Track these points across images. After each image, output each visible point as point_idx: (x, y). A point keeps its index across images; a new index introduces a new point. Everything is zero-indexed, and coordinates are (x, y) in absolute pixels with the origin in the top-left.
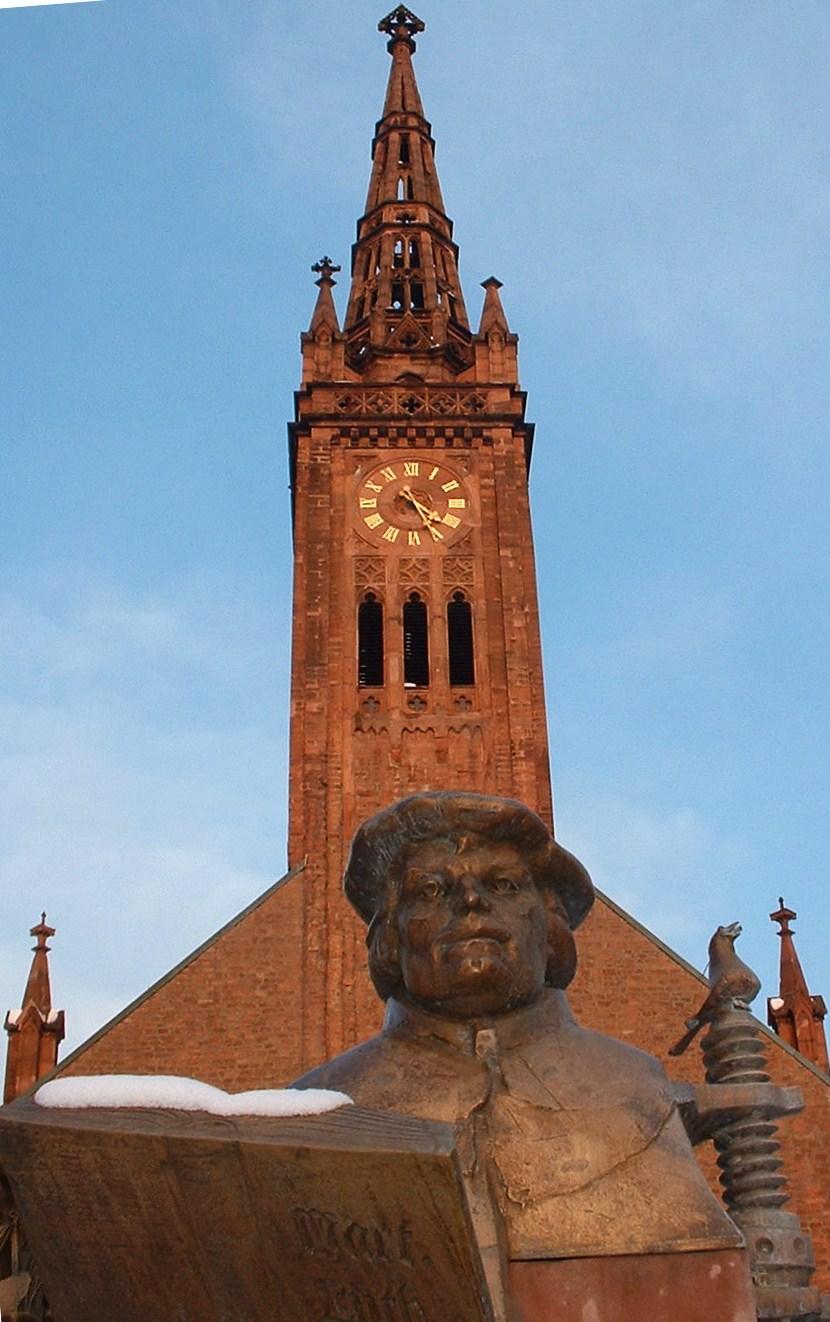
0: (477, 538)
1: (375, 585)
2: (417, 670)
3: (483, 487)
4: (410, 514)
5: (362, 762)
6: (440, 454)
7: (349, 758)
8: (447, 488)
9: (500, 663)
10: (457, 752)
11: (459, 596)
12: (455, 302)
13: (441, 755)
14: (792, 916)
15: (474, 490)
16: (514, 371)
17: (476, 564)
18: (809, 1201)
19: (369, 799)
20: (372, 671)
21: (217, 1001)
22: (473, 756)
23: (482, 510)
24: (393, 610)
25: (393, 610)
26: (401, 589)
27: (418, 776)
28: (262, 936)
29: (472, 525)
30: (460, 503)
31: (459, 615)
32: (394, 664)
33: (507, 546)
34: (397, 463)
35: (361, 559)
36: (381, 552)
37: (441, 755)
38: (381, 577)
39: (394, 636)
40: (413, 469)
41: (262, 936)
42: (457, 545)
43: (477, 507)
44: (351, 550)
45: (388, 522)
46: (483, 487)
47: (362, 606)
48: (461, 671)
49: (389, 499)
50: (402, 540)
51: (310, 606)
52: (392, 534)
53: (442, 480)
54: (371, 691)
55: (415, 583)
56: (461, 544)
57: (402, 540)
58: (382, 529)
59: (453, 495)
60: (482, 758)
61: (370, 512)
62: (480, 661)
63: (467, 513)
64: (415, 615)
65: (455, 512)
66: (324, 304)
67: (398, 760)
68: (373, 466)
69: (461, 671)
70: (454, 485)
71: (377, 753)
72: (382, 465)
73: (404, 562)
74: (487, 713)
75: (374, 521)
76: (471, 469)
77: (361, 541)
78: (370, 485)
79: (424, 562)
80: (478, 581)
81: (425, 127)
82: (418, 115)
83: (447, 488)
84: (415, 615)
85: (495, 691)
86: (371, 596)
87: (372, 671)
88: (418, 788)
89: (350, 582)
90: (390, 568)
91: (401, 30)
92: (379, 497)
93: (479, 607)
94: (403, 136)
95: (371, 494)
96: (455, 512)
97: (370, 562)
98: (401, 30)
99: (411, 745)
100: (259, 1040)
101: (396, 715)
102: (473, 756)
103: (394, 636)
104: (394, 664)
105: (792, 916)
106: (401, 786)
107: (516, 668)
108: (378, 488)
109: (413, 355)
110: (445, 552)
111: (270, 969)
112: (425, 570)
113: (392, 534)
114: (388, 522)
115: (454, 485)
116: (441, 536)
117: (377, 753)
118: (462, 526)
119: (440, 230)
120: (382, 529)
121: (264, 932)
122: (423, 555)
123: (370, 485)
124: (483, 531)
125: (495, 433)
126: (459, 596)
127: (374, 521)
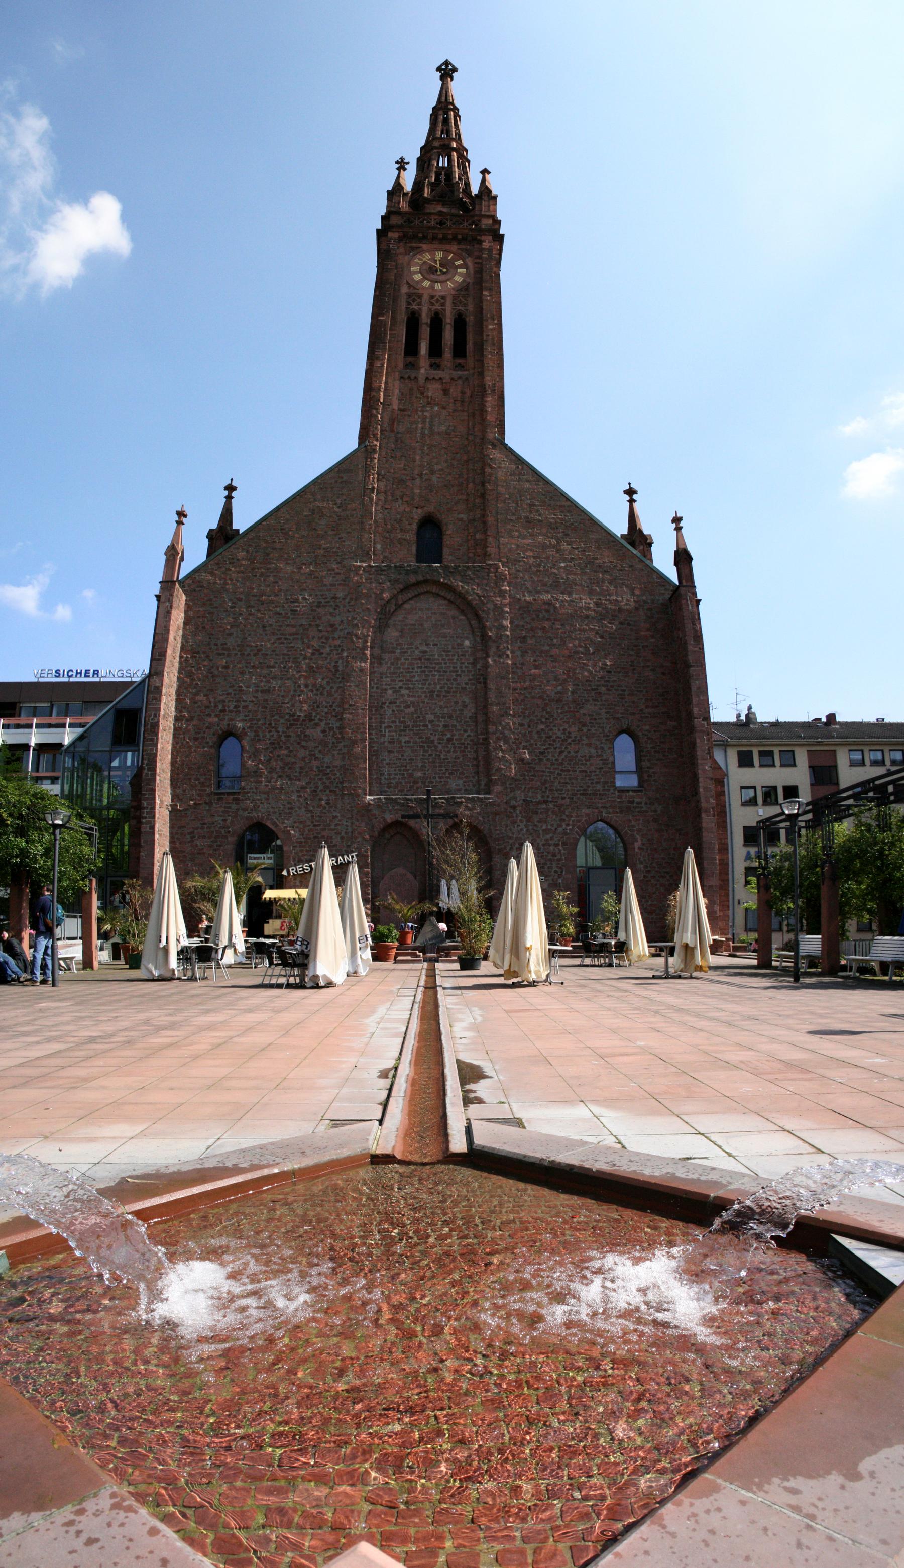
1: (416, 308)
2: (435, 350)
4: (436, 278)
5: (402, 394)
6: (454, 247)
7: (397, 392)
8: (457, 263)
9: (480, 348)
10: (454, 391)
12: (467, 185)
13: (446, 392)
14: (635, 492)
15: (470, 264)
16: (495, 211)
18: (643, 633)
19: (406, 413)
20: (411, 349)
21: (313, 514)
22: (463, 393)
24: (425, 318)
25: (425, 318)
26: (430, 310)
27: (433, 402)
28: (340, 481)
31: (460, 324)
32: (424, 348)
33: (486, 290)
34: (432, 251)
35: (409, 295)
36: (420, 292)
38: (419, 304)
39: (425, 332)
40: (439, 255)
41: (340, 481)
42: (461, 290)
44: (404, 290)
45: (425, 278)
47: (408, 318)
48: (459, 350)
49: (425, 267)
50: (432, 287)
52: (426, 284)
55: (437, 307)
56: (463, 289)
57: (432, 287)
58: (421, 281)
59: (460, 267)
60: (468, 393)
61: (416, 273)
62: (470, 346)
64: (437, 322)
67: (422, 394)
68: (418, 251)
69: (459, 350)
70: (460, 262)
71: (411, 390)
72: (423, 251)
73: (432, 297)
74: (471, 371)
75: (418, 277)
76: (469, 255)
77: (409, 286)
79: (443, 298)
80: (471, 308)
81: (456, 109)
82: (452, 103)
83: (457, 263)
84: (437, 322)
85: (477, 361)
87: (411, 349)
88: (432, 408)
89: (403, 305)
92: (421, 266)
93: (470, 319)
94: (444, 112)
95: (416, 265)
96: (461, 275)
97: (414, 296)
99: (429, 386)
100: (336, 535)
101: (422, 371)
103: (425, 332)
104: (424, 348)
105: (635, 492)
106: (423, 407)
107: (489, 348)
110: (453, 293)
111: (344, 497)
115: (460, 262)
117: (411, 390)
118: (463, 281)
119: (462, 152)
120: (421, 281)
121: (342, 478)
122: (443, 294)
127: (418, 277)
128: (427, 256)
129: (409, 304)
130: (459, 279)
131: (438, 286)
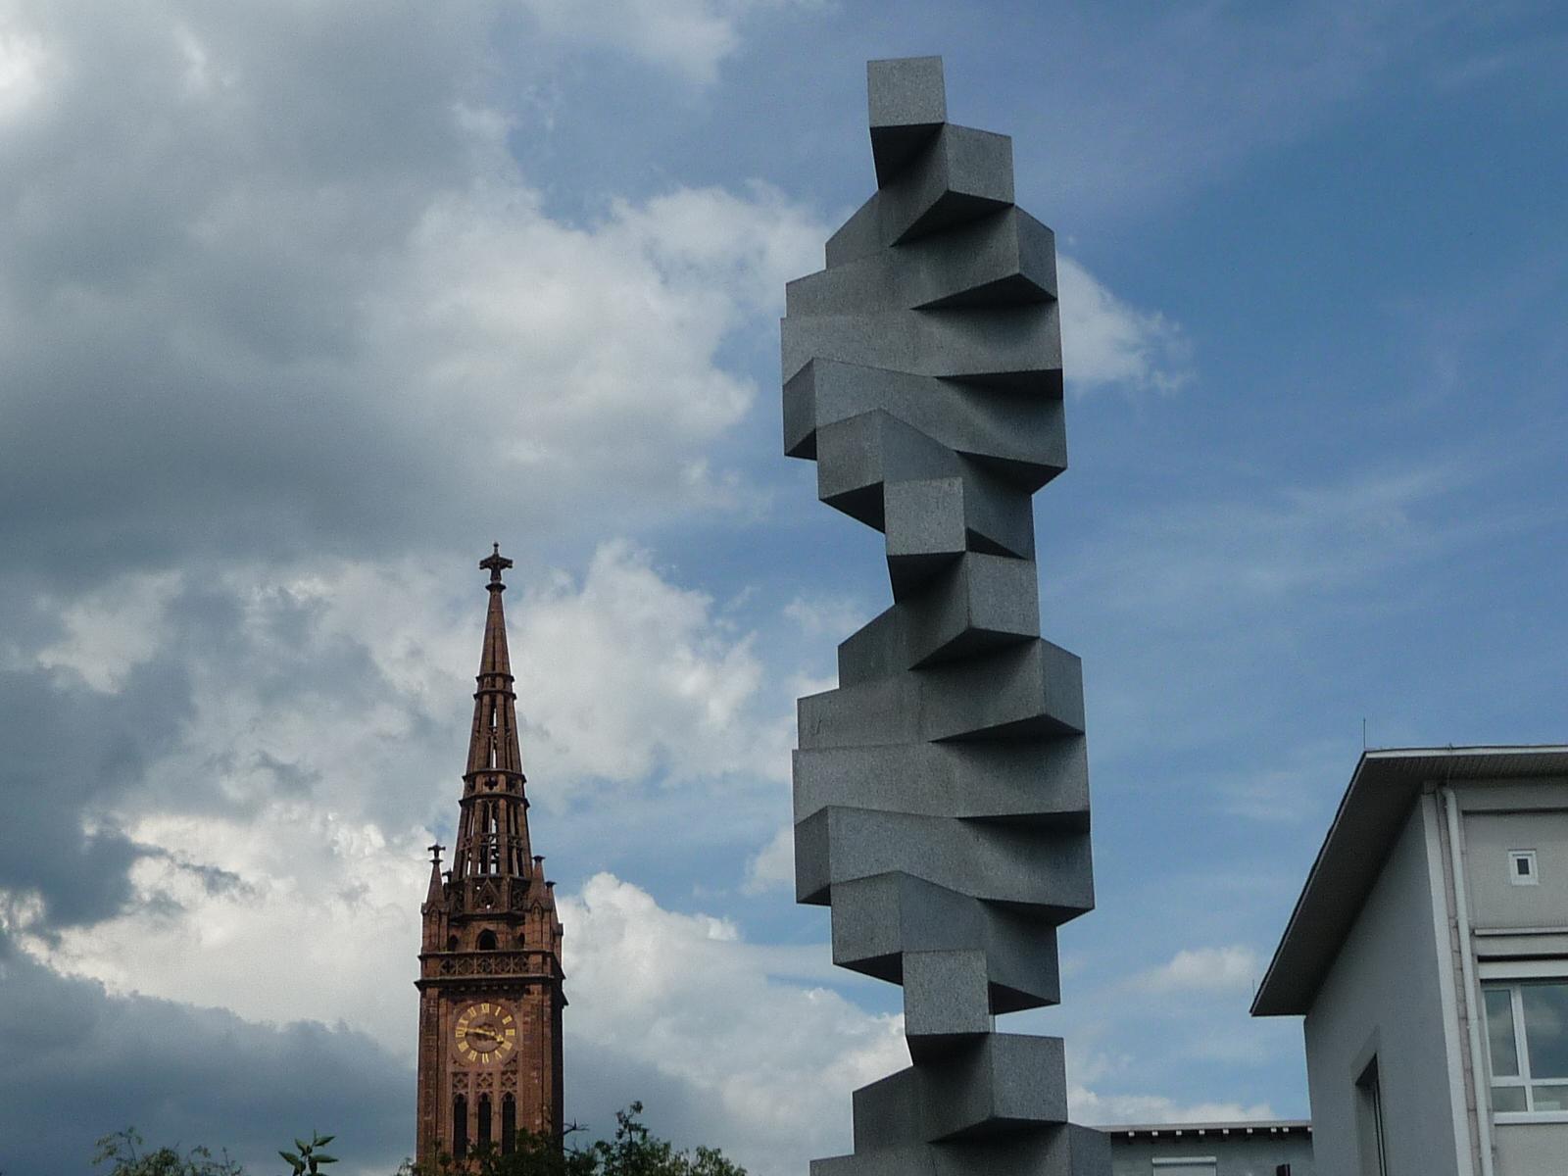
0: (520, 1059)
1: (463, 1092)
3: (525, 1023)
6: (502, 1001)
8: (505, 1021)
17: (519, 1076)
23: (524, 1040)
24: (472, 1108)
25: (472, 1108)
26: (477, 1093)
29: (517, 1049)
30: (511, 1032)
33: (534, 1069)
36: (466, 1070)
40: (485, 1008)
42: (509, 1063)
44: (450, 1068)
45: (471, 1047)
46: (525, 1023)
50: (479, 1059)
51: (427, 1114)
52: (473, 1055)
53: (502, 1016)
57: (479, 1059)
58: (467, 1052)
59: (508, 1026)
63: (515, 1040)
65: (509, 1039)
66: (436, 873)
70: (509, 1018)
73: (479, 1075)
79: (490, 1074)
80: (519, 1087)
83: (505, 1021)
86: (461, 1097)
90: (471, 1079)
93: (519, 1105)
96: (509, 1039)
97: (460, 1076)
109: (489, 917)
110: (502, 1068)
112: (490, 1081)
113: (473, 1055)
114: (471, 1047)
115: (507, 1020)
116: (500, 1056)
120: (467, 1052)
122: (490, 1070)
123: (461, 1021)
124: (524, 1053)
125: (532, 988)
127: (463, 1046)
129: (455, 1086)
130: (507, 1046)
131: (485, 1058)
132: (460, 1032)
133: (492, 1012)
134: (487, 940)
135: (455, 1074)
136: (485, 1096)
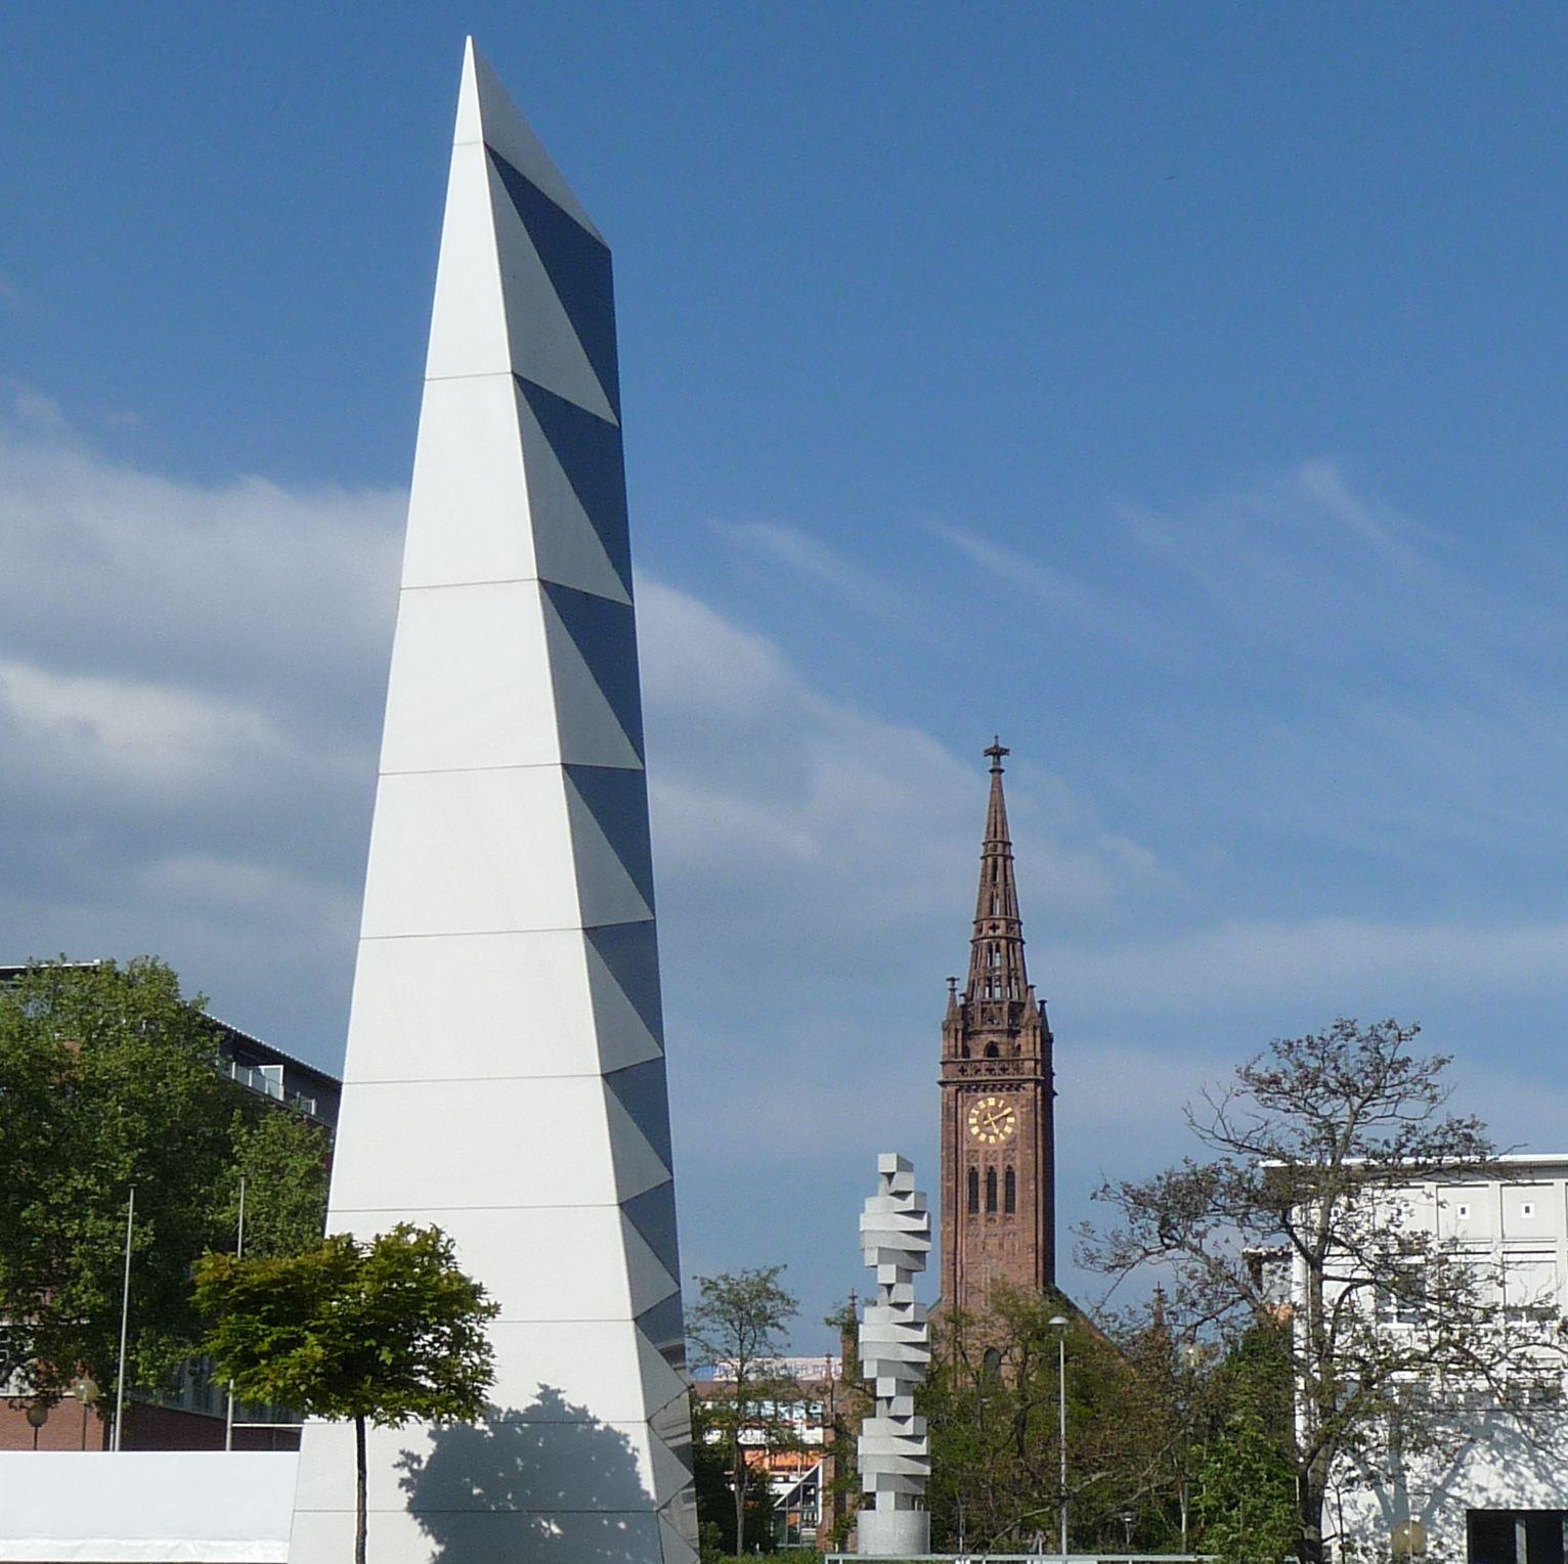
0: (1018, 1139)
1: (975, 1165)
2: (991, 1206)
11: (1009, 1167)
13: (1001, 1245)
15: (1017, 1113)
37: (1001, 1245)
39: (982, 1189)
40: (992, 1101)
43: (1019, 1122)
48: (1009, 1207)
54: (973, 1215)
58: (979, 1134)
64: (991, 1173)
78: (973, 1111)
80: (1018, 1162)
84: (991, 1173)
86: (973, 1168)
87: (973, 1206)
91: (997, 737)
95: (974, 1116)
96: (1010, 1125)
98: (997, 737)
102: (1013, 1245)
103: (982, 1189)
108: (977, 1112)
113: (983, 1137)
118: (1013, 1133)
123: (973, 1111)
126: (1009, 1167)
127: (975, 1130)
128: (981, 1104)
130: (1008, 1129)
132: (972, 1121)
133: (997, 1104)
134: (992, 1050)
135: (969, 1151)
136: (991, 1168)
